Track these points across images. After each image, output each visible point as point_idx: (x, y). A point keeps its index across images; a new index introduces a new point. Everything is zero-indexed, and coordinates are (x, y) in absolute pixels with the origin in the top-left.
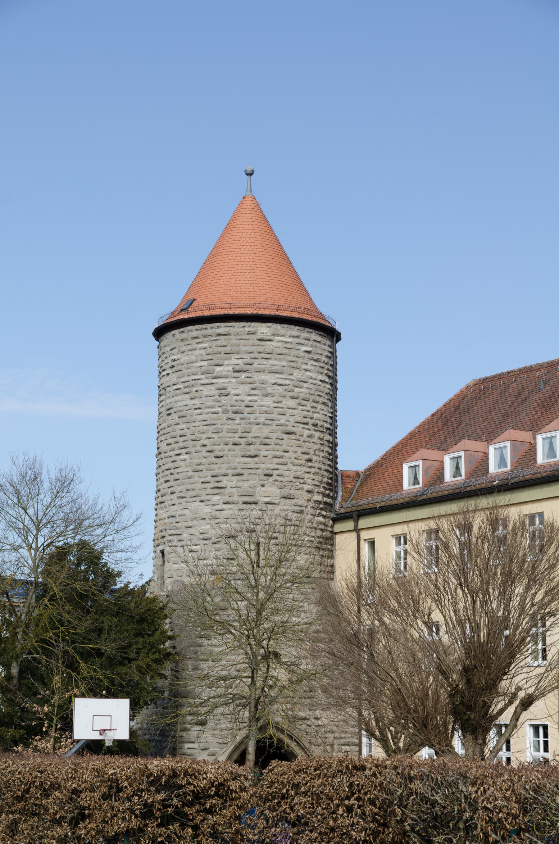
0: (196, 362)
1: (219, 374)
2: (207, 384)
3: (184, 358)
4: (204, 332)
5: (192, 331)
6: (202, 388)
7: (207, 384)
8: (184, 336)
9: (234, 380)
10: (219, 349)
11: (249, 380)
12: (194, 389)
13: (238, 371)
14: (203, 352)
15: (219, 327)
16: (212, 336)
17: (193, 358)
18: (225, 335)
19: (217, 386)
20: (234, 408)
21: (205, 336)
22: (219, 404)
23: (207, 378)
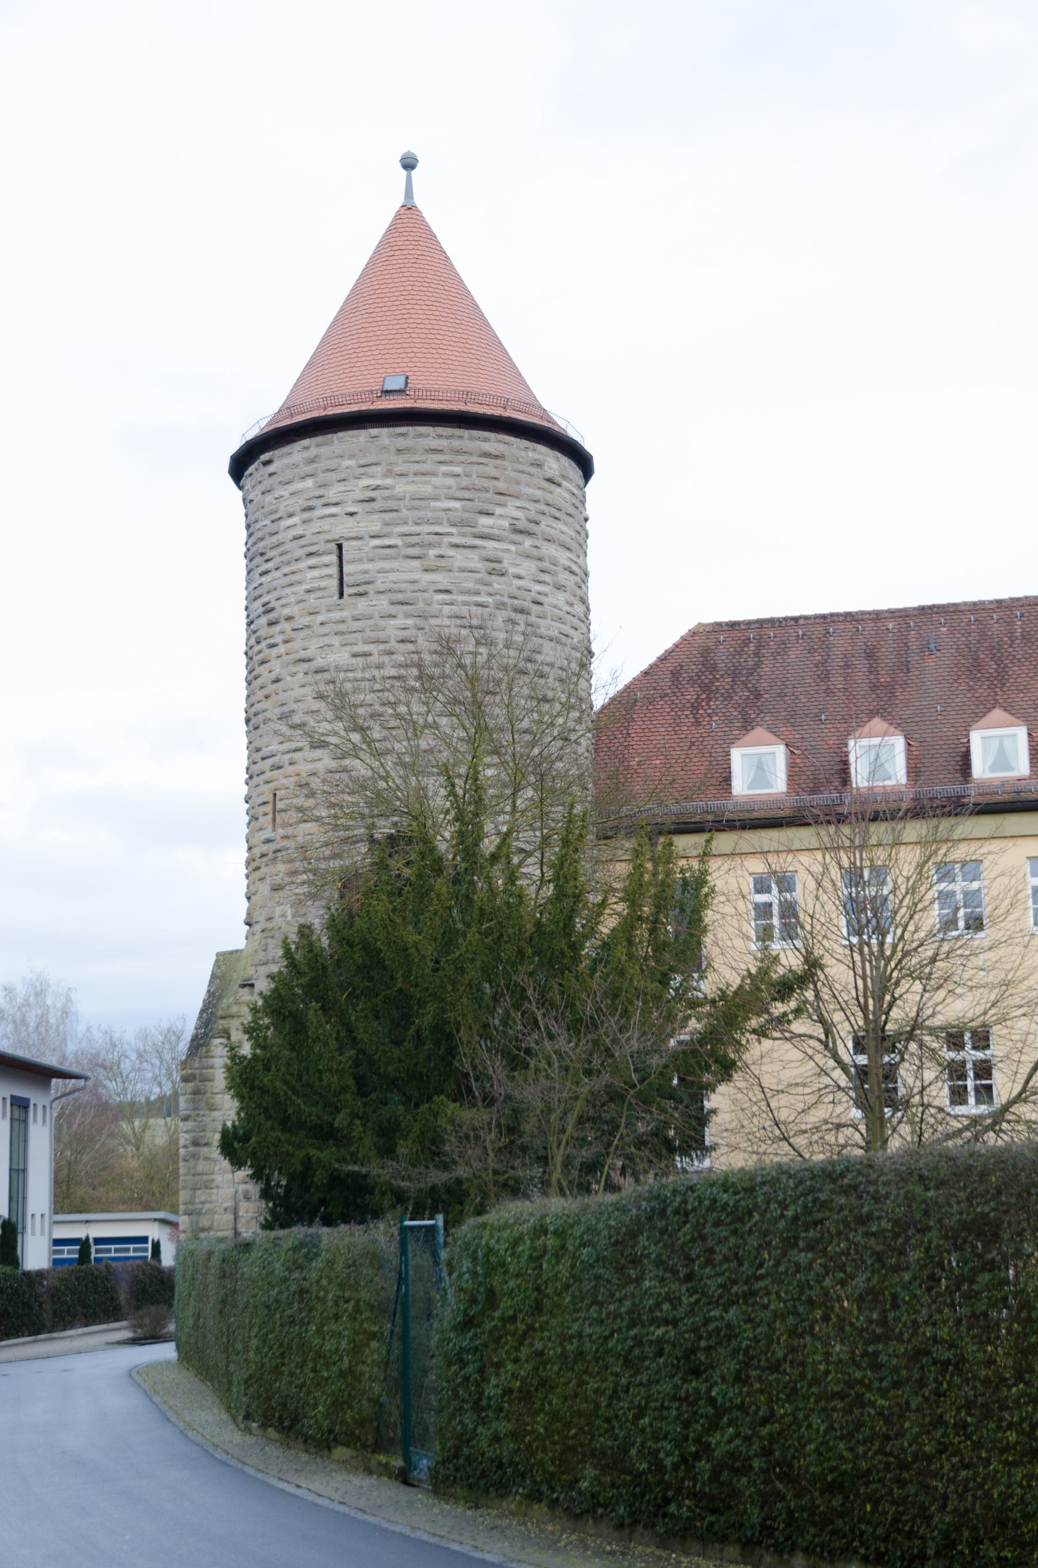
0: (436, 498)
1: (487, 531)
2: (464, 547)
3: (401, 487)
4: (456, 443)
5: (428, 436)
6: (451, 552)
7: (464, 547)
8: (402, 443)
9: (513, 548)
10: (486, 483)
11: (535, 552)
12: (433, 552)
13: (521, 532)
14: (451, 481)
15: (486, 440)
16: (471, 454)
17: (428, 490)
18: (496, 457)
19: (484, 553)
20: (516, 602)
21: (458, 452)
22: (489, 589)
23: (463, 535)
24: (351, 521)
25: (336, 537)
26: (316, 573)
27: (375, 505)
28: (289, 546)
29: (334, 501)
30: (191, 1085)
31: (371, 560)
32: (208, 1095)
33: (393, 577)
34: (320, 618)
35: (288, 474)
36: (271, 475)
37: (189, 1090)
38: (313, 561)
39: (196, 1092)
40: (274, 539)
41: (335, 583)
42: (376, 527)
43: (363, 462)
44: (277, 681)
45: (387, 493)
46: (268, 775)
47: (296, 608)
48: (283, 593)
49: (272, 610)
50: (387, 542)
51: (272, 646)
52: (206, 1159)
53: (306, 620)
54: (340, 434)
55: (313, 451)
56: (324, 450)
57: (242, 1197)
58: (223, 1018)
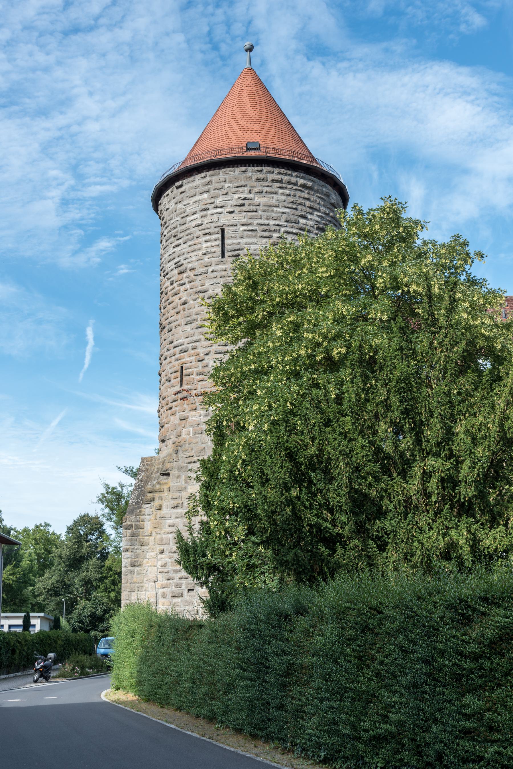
0: (278, 206)
3: (257, 199)
5: (273, 172)
12: (276, 235)
14: (284, 198)
17: (273, 202)
21: (289, 183)
24: (230, 216)
25: (221, 225)
26: (209, 244)
27: (244, 208)
28: (192, 230)
29: (220, 205)
30: (130, 531)
31: (242, 237)
32: (141, 537)
33: (253, 247)
34: (211, 269)
35: (192, 192)
36: (181, 193)
37: (128, 534)
38: (207, 238)
39: (133, 535)
40: (183, 227)
41: (219, 249)
42: (244, 221)
43: (236, 185)
44: (185, 303)
45: (250, 202)
46: (178, 356)
47: (197, 263)
48: (188, 256)
49: (182, 265)
50: (250, 228)
51: (182, 285)
52: (139, 574)
53: (203, 270)
54: (224, 170)
55: (208, 179)
56: (213, 178)
57: (160, 597)
58: (150, 492)
